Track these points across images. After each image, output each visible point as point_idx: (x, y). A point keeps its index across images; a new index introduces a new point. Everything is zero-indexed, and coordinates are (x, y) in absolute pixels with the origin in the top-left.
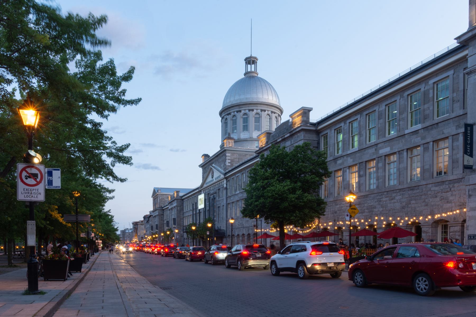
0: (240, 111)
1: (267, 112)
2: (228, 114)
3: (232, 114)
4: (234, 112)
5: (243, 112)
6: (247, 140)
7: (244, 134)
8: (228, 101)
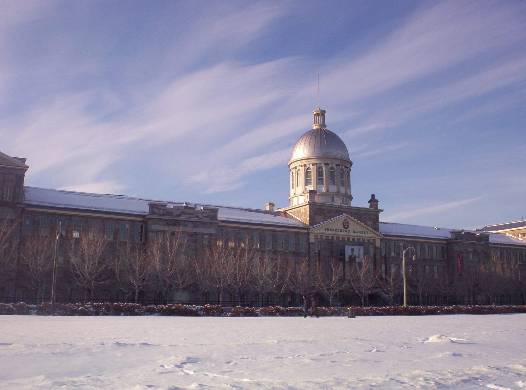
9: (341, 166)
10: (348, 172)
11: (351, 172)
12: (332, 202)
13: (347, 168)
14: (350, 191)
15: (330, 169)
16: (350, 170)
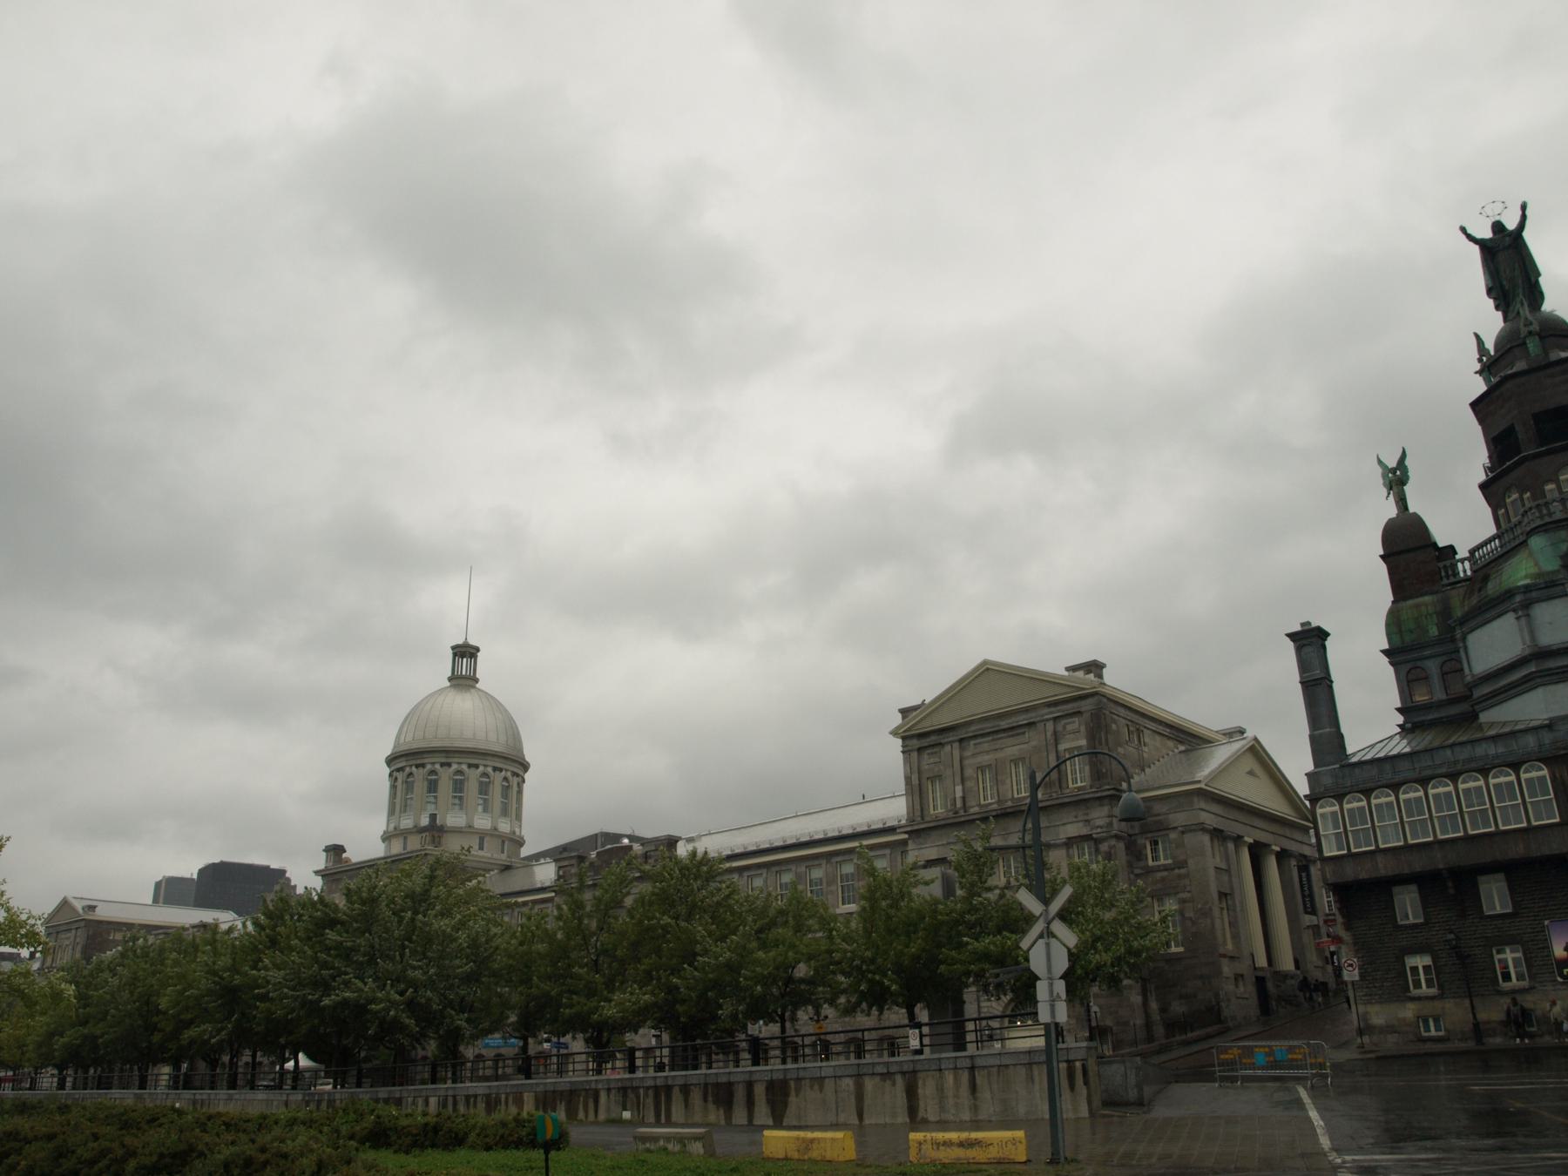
0: (449, 765)
1: (481, 768)
2: (398, 770)
3: (408, 769)
4: (411, 766)
5: (429, 767)
6: (461, 832)
7: (455, 817)
8: (409, 738)
9: (504, 773)
10: (518, 784)
11: (525, 785)
12: (480, 849)
13: (518, 775)
14: (520, 826)
15: (480, 777)
16: (524, 781)
